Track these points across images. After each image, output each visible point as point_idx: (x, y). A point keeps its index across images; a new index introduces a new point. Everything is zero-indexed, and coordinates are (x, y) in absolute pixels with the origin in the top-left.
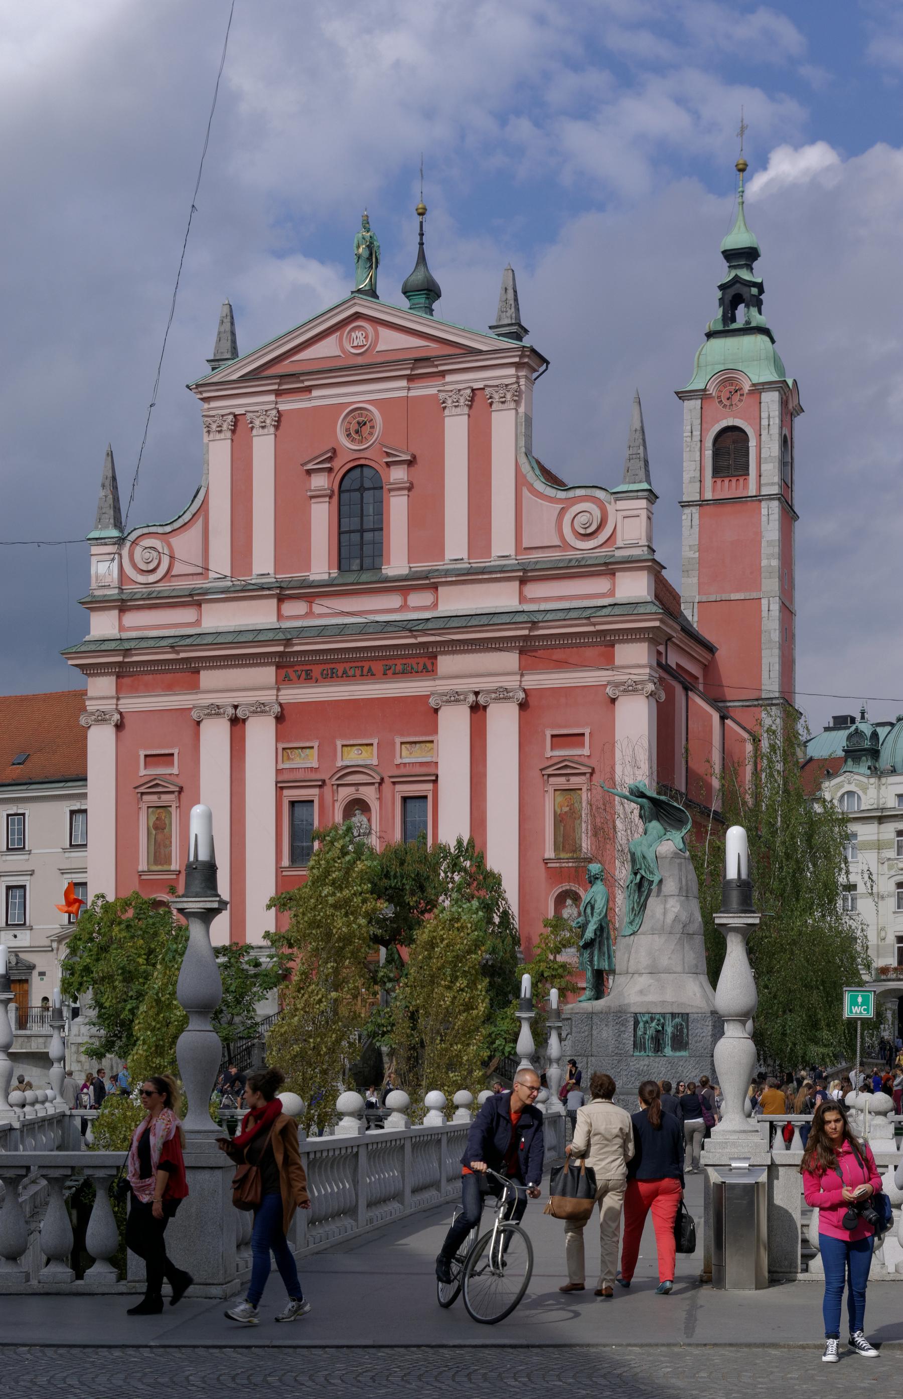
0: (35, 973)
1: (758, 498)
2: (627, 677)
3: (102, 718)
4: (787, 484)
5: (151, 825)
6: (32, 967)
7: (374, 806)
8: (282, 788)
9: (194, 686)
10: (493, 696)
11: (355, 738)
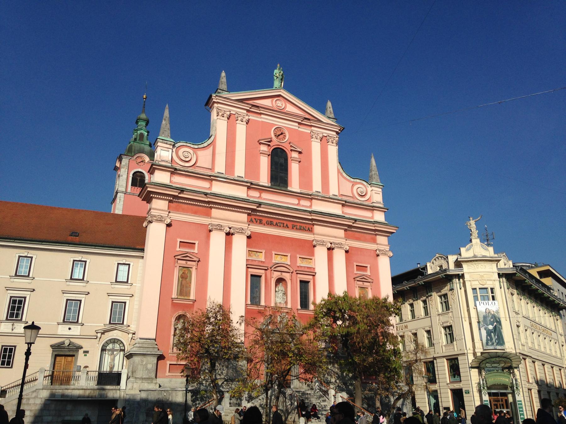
0: (81, 351)
2: (384, 249)
5: (180, 276)
8: (248, 268)
9: (208, 215)
10: (336, 245)
11: (280, 252)
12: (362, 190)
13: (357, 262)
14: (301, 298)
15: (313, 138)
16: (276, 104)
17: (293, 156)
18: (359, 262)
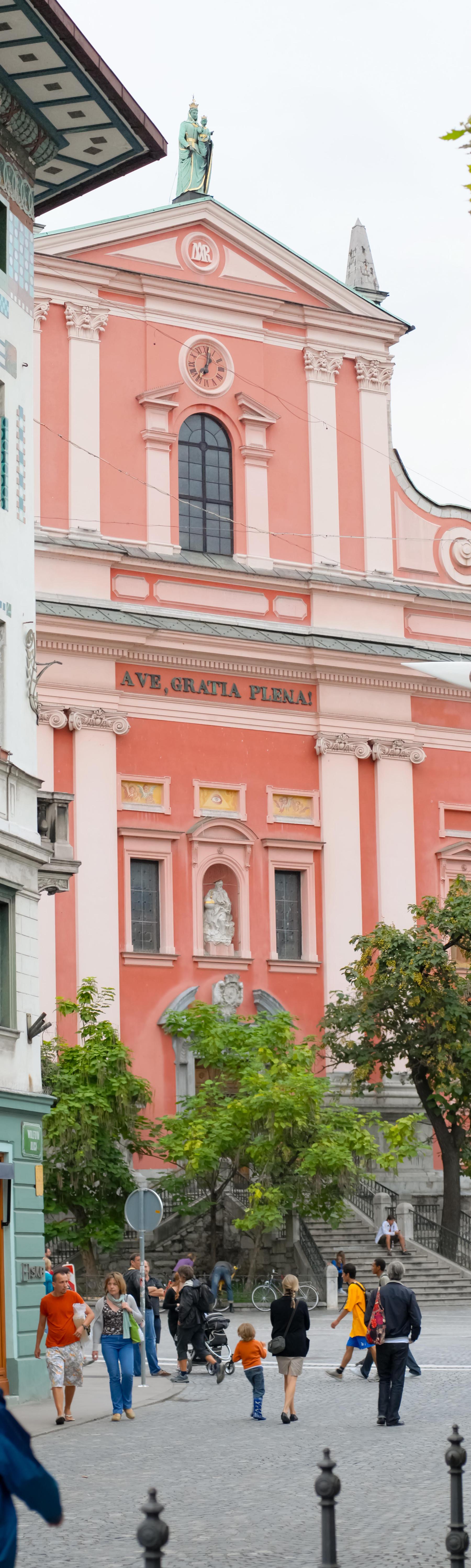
10: (387, 749)
11: (216, 780)
14: (279, 924)
15: (310, 370)
16: (191, 256)
17: (248, 444)
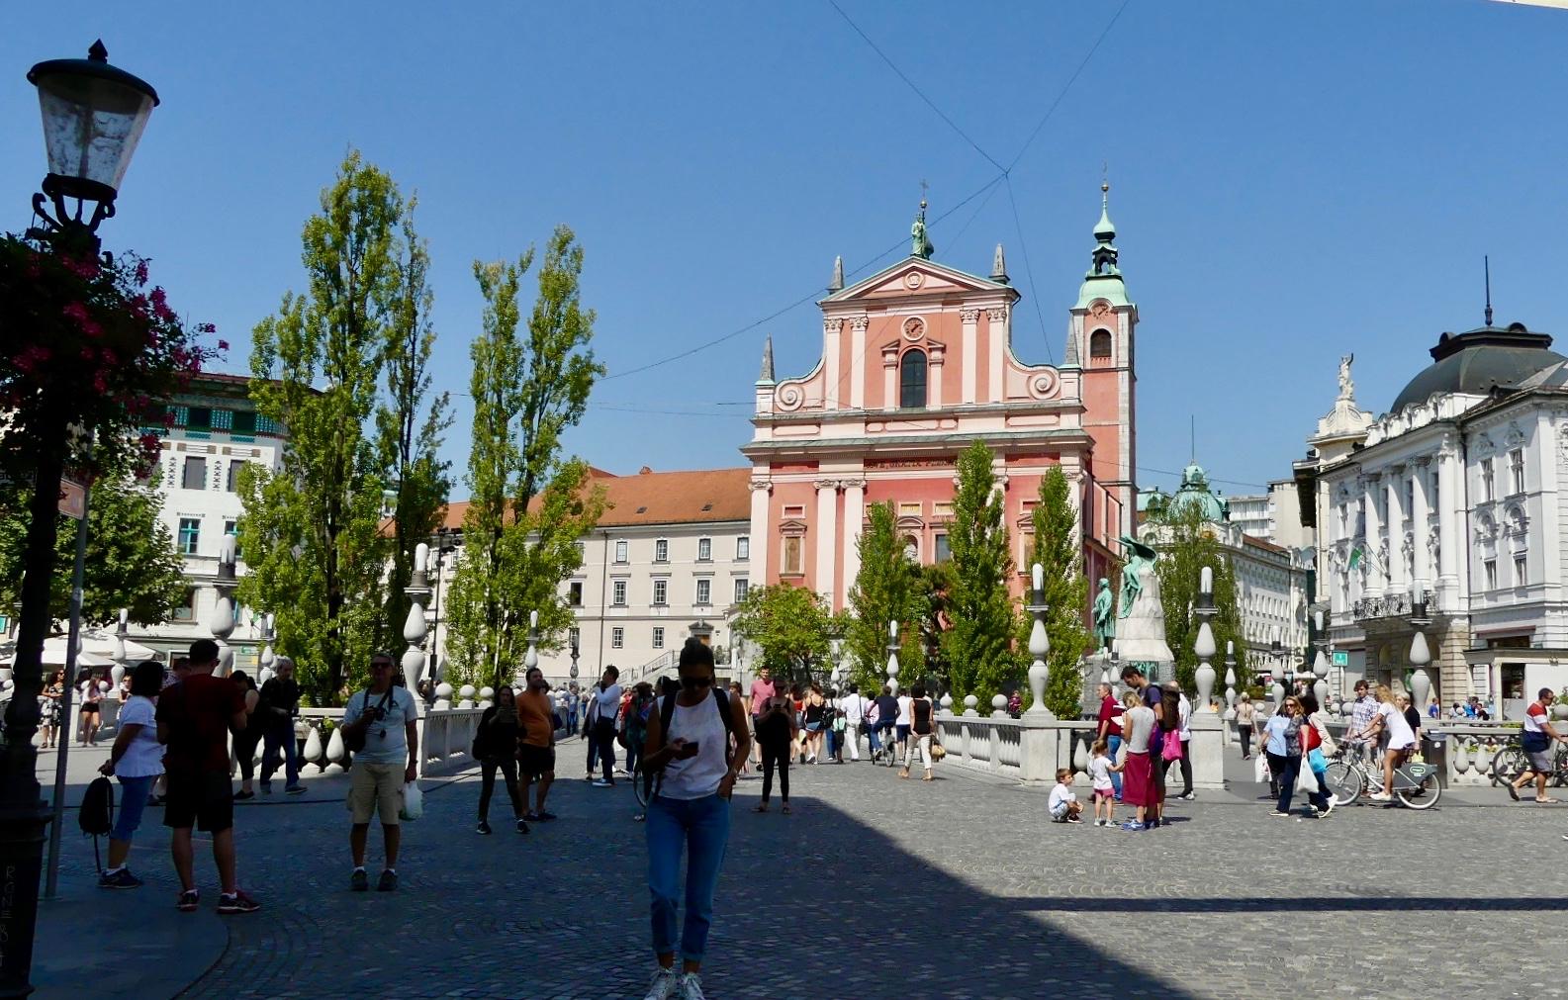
0: (714, 632)
1: (1116, 370)
3: (760, 487)
4: (1131, 361)
6: (711, 628)
7: (920, 541)
11: (908, 500)
12: (1042, 382)
13: (1024, 497)
18: (1028, 497)
